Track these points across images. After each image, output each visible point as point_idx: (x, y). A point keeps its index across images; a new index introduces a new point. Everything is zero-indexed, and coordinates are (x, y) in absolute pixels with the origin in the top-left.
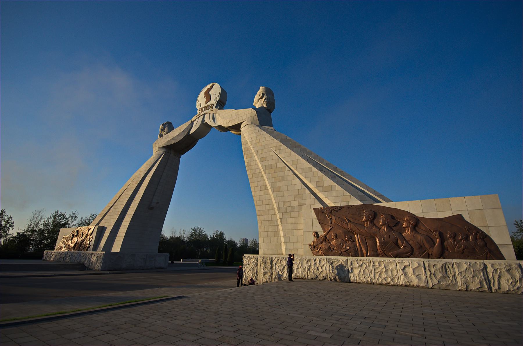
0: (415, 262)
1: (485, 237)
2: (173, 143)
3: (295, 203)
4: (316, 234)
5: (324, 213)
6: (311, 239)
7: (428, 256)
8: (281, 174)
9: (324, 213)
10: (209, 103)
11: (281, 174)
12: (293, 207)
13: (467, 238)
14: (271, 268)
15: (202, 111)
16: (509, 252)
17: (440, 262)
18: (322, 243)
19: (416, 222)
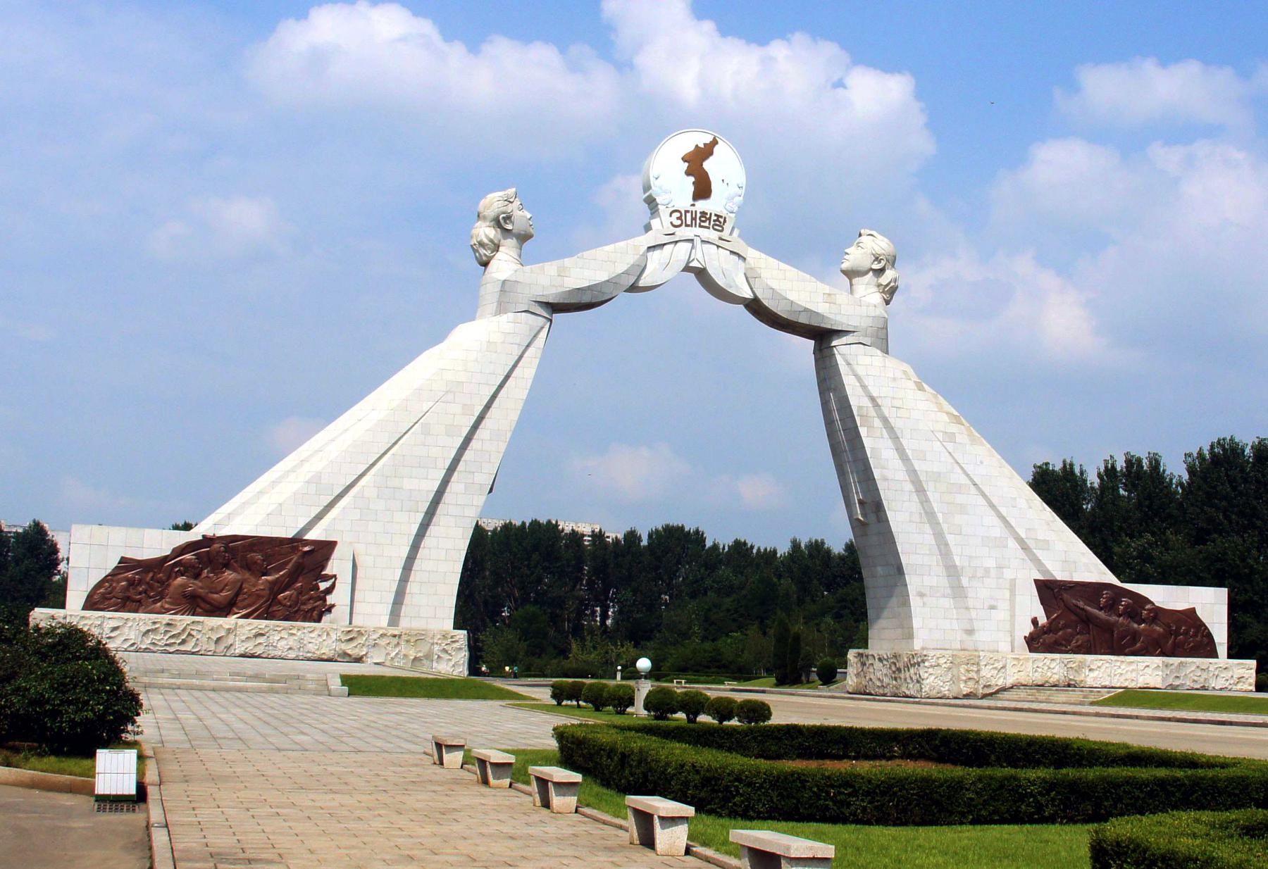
0: (1157, 661)
1: (1209, 636)
2: (586, 299)
3: (991, 563)
4: (1035, 622)
5: (1049, 590)
6: (1028, 629)
7: (1163, 654)
8: (960, 499)
9: (1049, 590)
10: (702, 205)
11: (960, 499)
12: (987, 570)
13: (1195, 635)
14: (978, 671)
15: (682, 223)
16: (1222, 649)
17: (1175, 661)
18: (1045, 633)
19: (1159, 614)
